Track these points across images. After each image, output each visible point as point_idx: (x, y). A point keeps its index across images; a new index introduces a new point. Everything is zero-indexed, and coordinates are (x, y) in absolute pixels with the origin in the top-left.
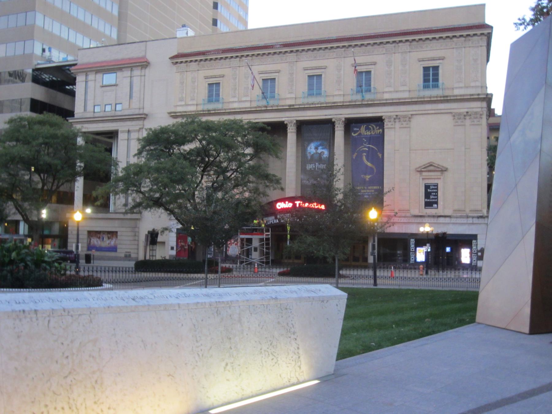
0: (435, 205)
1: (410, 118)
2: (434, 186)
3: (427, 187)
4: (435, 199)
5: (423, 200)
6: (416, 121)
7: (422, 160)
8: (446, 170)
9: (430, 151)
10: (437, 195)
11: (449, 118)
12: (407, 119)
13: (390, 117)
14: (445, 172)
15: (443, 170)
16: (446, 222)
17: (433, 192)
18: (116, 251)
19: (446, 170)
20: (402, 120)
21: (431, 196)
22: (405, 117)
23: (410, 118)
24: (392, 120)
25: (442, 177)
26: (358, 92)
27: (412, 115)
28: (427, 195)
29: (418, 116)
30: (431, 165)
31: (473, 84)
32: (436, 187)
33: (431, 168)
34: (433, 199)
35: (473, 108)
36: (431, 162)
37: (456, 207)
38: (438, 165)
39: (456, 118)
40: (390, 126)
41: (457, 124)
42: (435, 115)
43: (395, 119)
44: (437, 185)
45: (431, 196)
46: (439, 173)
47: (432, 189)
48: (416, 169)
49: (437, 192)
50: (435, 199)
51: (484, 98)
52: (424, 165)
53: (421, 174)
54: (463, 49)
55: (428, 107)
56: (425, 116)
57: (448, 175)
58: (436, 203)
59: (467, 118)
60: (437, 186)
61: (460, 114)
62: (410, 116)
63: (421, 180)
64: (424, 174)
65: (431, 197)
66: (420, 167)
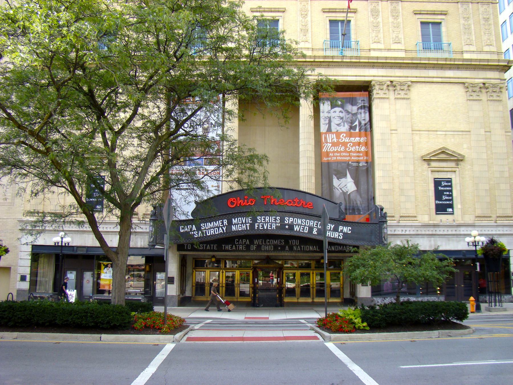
0: (450, 210)
1: (409, 86)
2: (447, 182)
3: (437, 183)
4: (449, 200)
5: (432, 202)
6: (417, 91)
7: (430, 145)
9: (438, 133)
10: (451, 195)
11: (459, 90)
12: (405, 87)
13: (381, 84)
14: (461, 163)
15: (458, 160)
17: (446, 191)
20: (398, 88)
21: (443, 198)
22: (402, 84)
23: (409, 86)
24: (385, 87)
25: (457, 169)
26: (332, 47)
27: (412, 82)
28: (438, 195)
29: (419, 85)
30: (443, 152)
31: (486, 49)
33: (443, 156)
34: (446, 200)
35: (490, 79)
36: (444, 148)
37: (479, 212)
38: (453, 152)
39: (470, 89)
41: (471, 98)
42: (442, 86)
43: (388, 86)
44: (450, 181)
45: (443, 198)
46: (453, 164)
47: (445, 186)
48: (422, 157)
49: (451, 191)
50: (449, 200)
52: (434, 151)
53: (429, 165)
54: (470, 5)
55: (432, 73)
57: (465, 166)
58: (451, 206)
60: (450, 181)
61: (473, 85)
62: (410, 83)
63: (430, 172)
64: (433, 164)
65: (444, 198)
66: (428, 154)
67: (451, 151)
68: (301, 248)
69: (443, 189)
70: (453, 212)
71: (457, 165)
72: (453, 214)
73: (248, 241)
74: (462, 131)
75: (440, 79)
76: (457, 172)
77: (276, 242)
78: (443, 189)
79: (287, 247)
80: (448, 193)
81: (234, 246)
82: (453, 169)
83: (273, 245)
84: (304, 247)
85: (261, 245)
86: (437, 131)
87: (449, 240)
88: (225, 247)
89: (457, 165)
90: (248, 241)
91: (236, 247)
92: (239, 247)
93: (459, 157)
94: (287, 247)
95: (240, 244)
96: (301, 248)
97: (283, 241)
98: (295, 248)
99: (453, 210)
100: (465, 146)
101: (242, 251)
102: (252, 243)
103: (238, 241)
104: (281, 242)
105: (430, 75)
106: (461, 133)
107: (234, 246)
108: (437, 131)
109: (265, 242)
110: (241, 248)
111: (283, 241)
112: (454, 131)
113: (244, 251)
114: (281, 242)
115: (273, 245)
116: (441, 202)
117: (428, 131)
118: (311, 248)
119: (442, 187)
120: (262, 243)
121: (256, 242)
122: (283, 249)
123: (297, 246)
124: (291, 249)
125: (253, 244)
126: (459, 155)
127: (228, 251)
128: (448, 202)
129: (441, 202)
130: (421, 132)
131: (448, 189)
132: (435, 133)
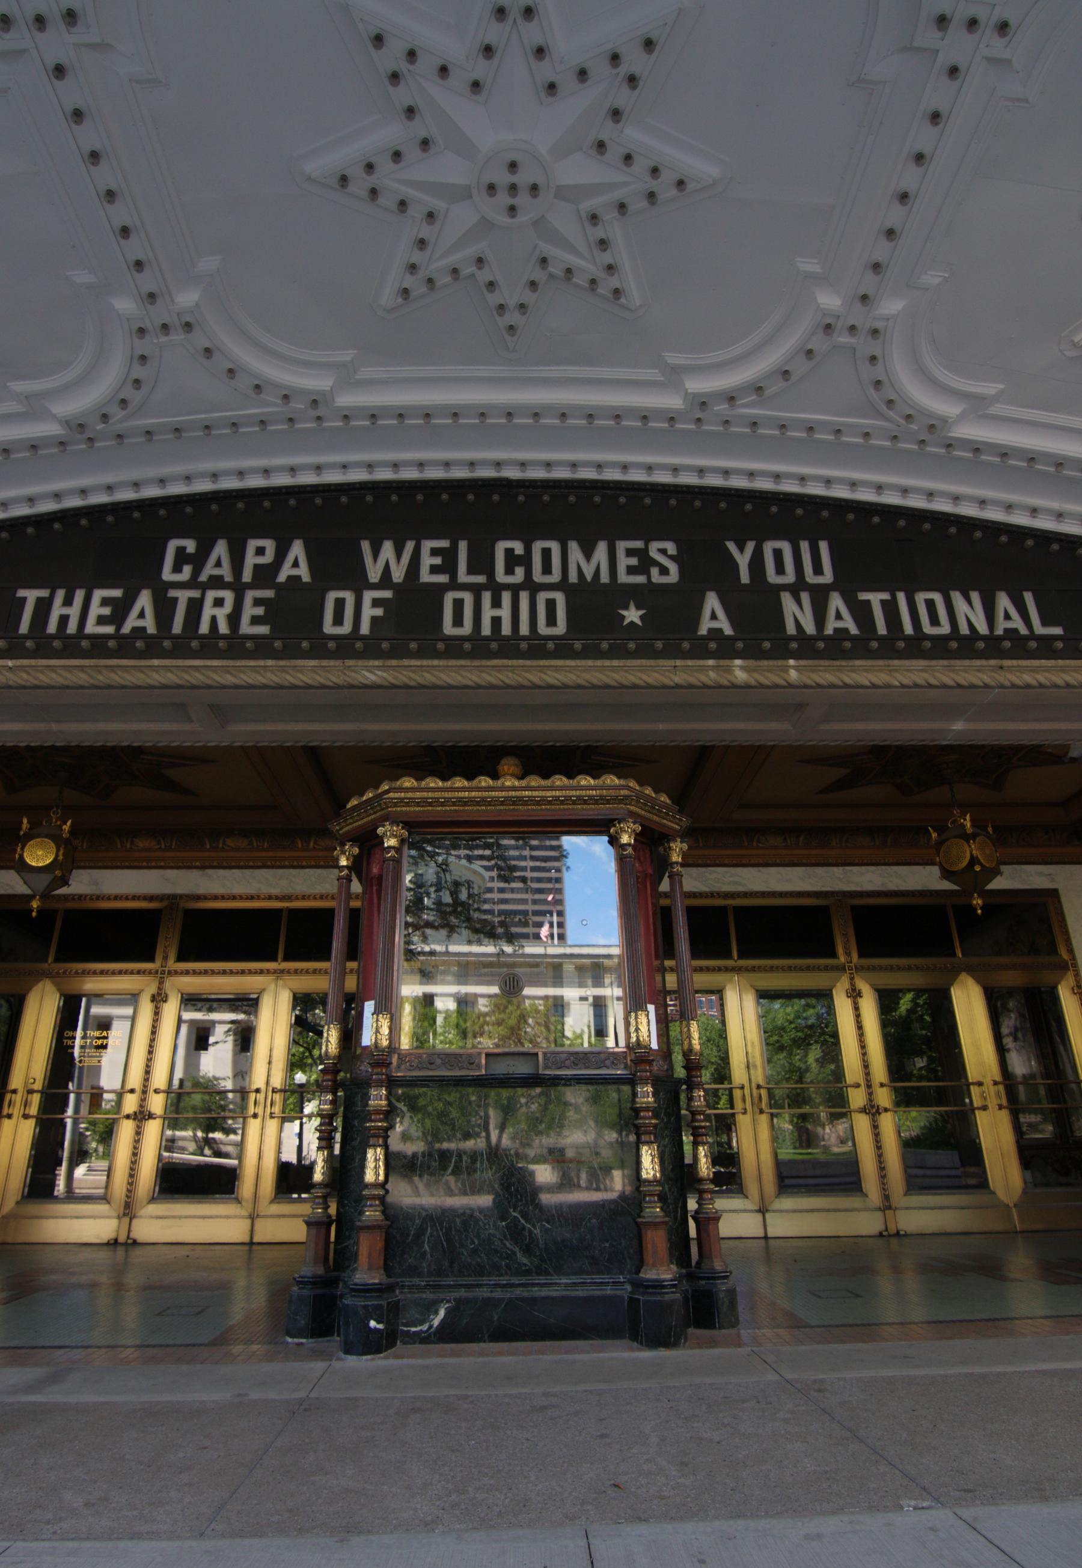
68: (862, 613)
73: (297, 549)
77: (592, 563)
79: (712, 602)
81: (144, 600)
83: (563, 585)
84: (890, 609)
85: (439, 590)
88: (43, 608)
90: (297, 549)
91: (164, 608)
92: (195, 608)
94: (712, 602)
95: (216, 582)
96: (862, 613)
97: (663, 550)
98: (796, 614)
101: (235, 646)
102: (339, 567)
103: (198, 560)
104: (645, 563)
107: (144, 600)
109: (481, 562)
110: (215, 614)
111: (663, 550)
113: (261, 648)
114: (645, 563)
115: (563, 585)
118: (970, 612)
120: (449, 565)
121: (385, 560)
122: (671, 625)
123: (820, 597)
124: (758, 626)
125: (358, 582)
127: (73, 645)
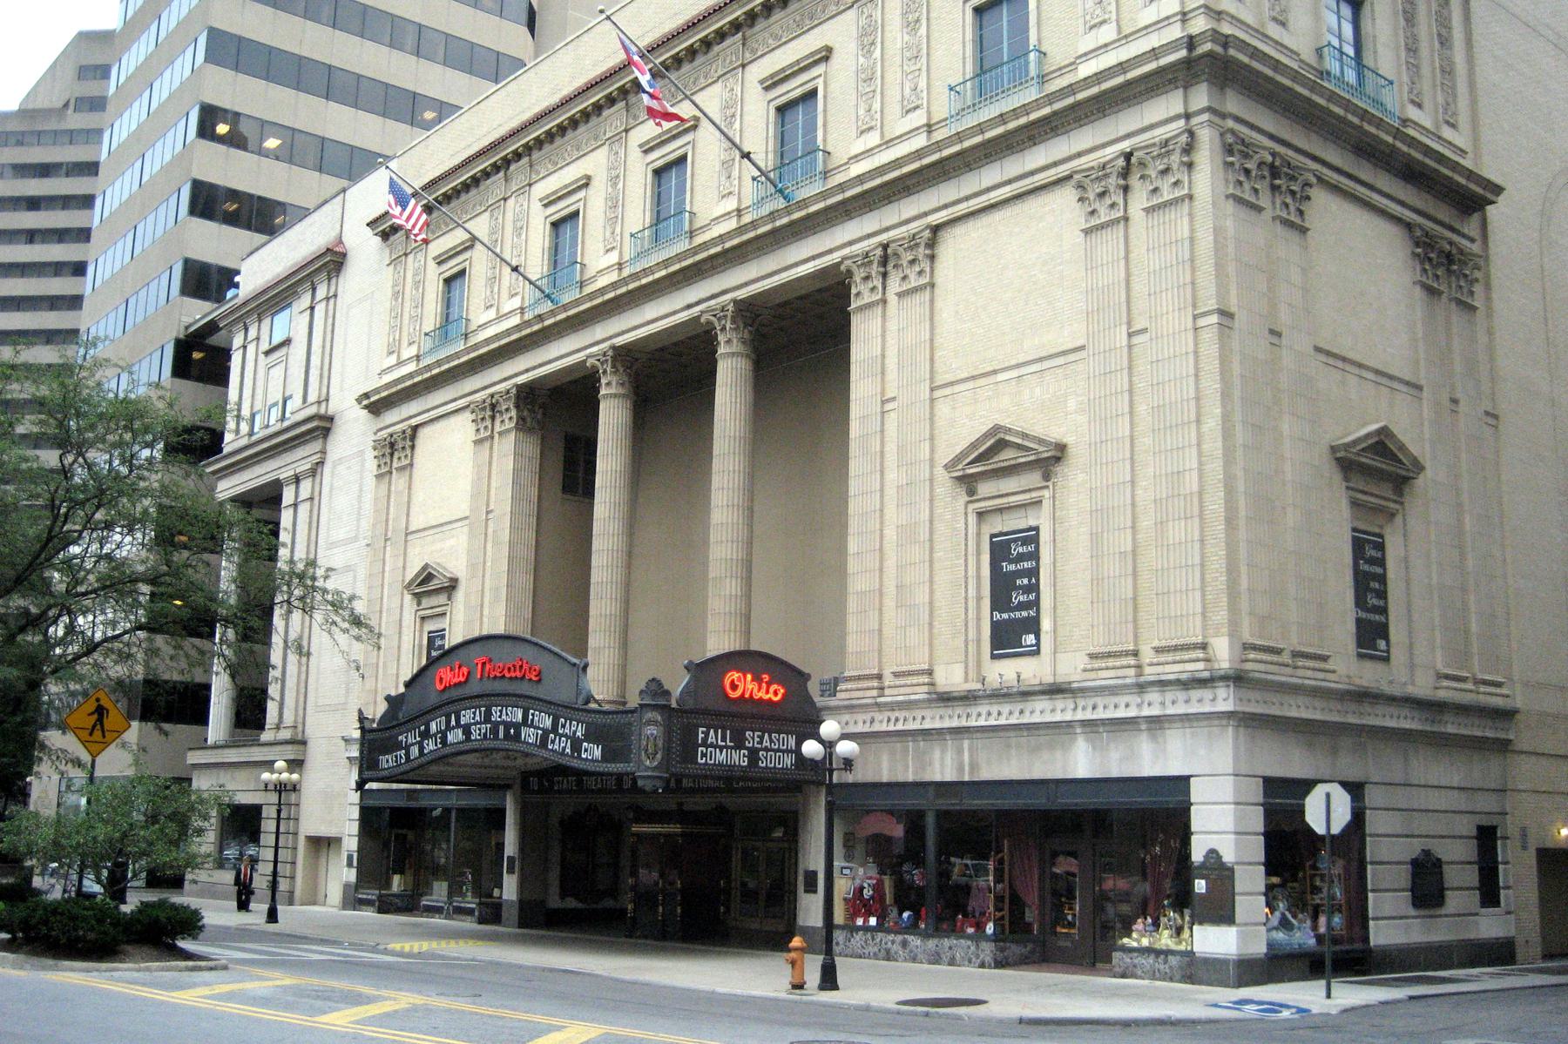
0: (1030, 639)
3: (999, 550)
7: (964, 425)
8: (1059, 453)
9: (1001, 377)
15: (1051, 460)
16: (1058, 717)
18: (806, 891)
19: (1059, 453)
25: (1046, 493)
32: (1031, 548)
36: (997, 429)
38: (1025, 436)
40: (867, 298)
41: (1094, 222)
46: (1034, 478)
51: (1187, 63)
52: (974, 446)
53: (971, 492)
55: (990, 175)
56: (985, 220)
57: (1075, 479)
58: (1033, 626)
59: (1134, 180)
63: (972, 519)
67: (1017, 433)
69: (1012, 567)
70: (1038, 644)
71: (1047, 477)
72: (1038, 652)
74: (1064, 353)
75: (1007, 189)
76: (1046, 504)
78: (1012, 567)
80: (1026, 581)
82: (1034, 494)
86: (995, 372)
87: (1009, 746)
89: (1047, 477)
93: (1041, 449)
99: (1038, 637)
100: (1072, 404)
105: (985, 185)
106: (1061, 360)
108: (995, 372)
112: (1041, 359)
116: (1005, 616)
117: (973, 378)
119: (1011, 561)
126: (1041, 441)
128: (1024, 614)
129: (1005, 616)
130: (957, 388)
131: (1027, 565)
132: (991, 379)
